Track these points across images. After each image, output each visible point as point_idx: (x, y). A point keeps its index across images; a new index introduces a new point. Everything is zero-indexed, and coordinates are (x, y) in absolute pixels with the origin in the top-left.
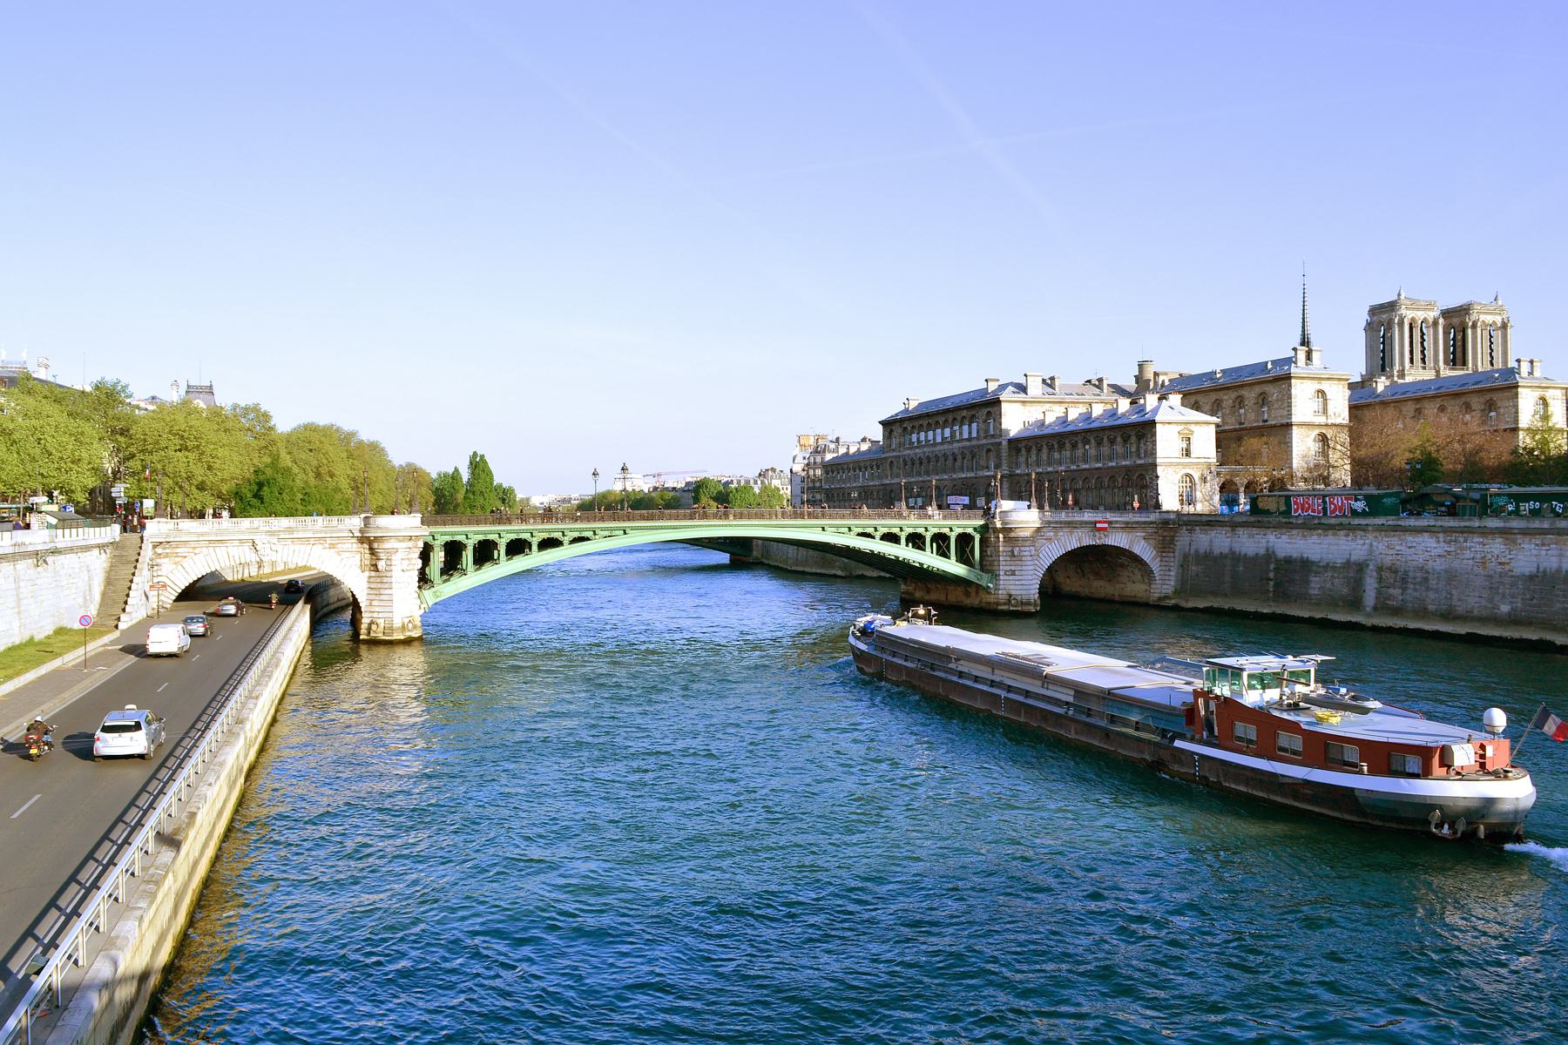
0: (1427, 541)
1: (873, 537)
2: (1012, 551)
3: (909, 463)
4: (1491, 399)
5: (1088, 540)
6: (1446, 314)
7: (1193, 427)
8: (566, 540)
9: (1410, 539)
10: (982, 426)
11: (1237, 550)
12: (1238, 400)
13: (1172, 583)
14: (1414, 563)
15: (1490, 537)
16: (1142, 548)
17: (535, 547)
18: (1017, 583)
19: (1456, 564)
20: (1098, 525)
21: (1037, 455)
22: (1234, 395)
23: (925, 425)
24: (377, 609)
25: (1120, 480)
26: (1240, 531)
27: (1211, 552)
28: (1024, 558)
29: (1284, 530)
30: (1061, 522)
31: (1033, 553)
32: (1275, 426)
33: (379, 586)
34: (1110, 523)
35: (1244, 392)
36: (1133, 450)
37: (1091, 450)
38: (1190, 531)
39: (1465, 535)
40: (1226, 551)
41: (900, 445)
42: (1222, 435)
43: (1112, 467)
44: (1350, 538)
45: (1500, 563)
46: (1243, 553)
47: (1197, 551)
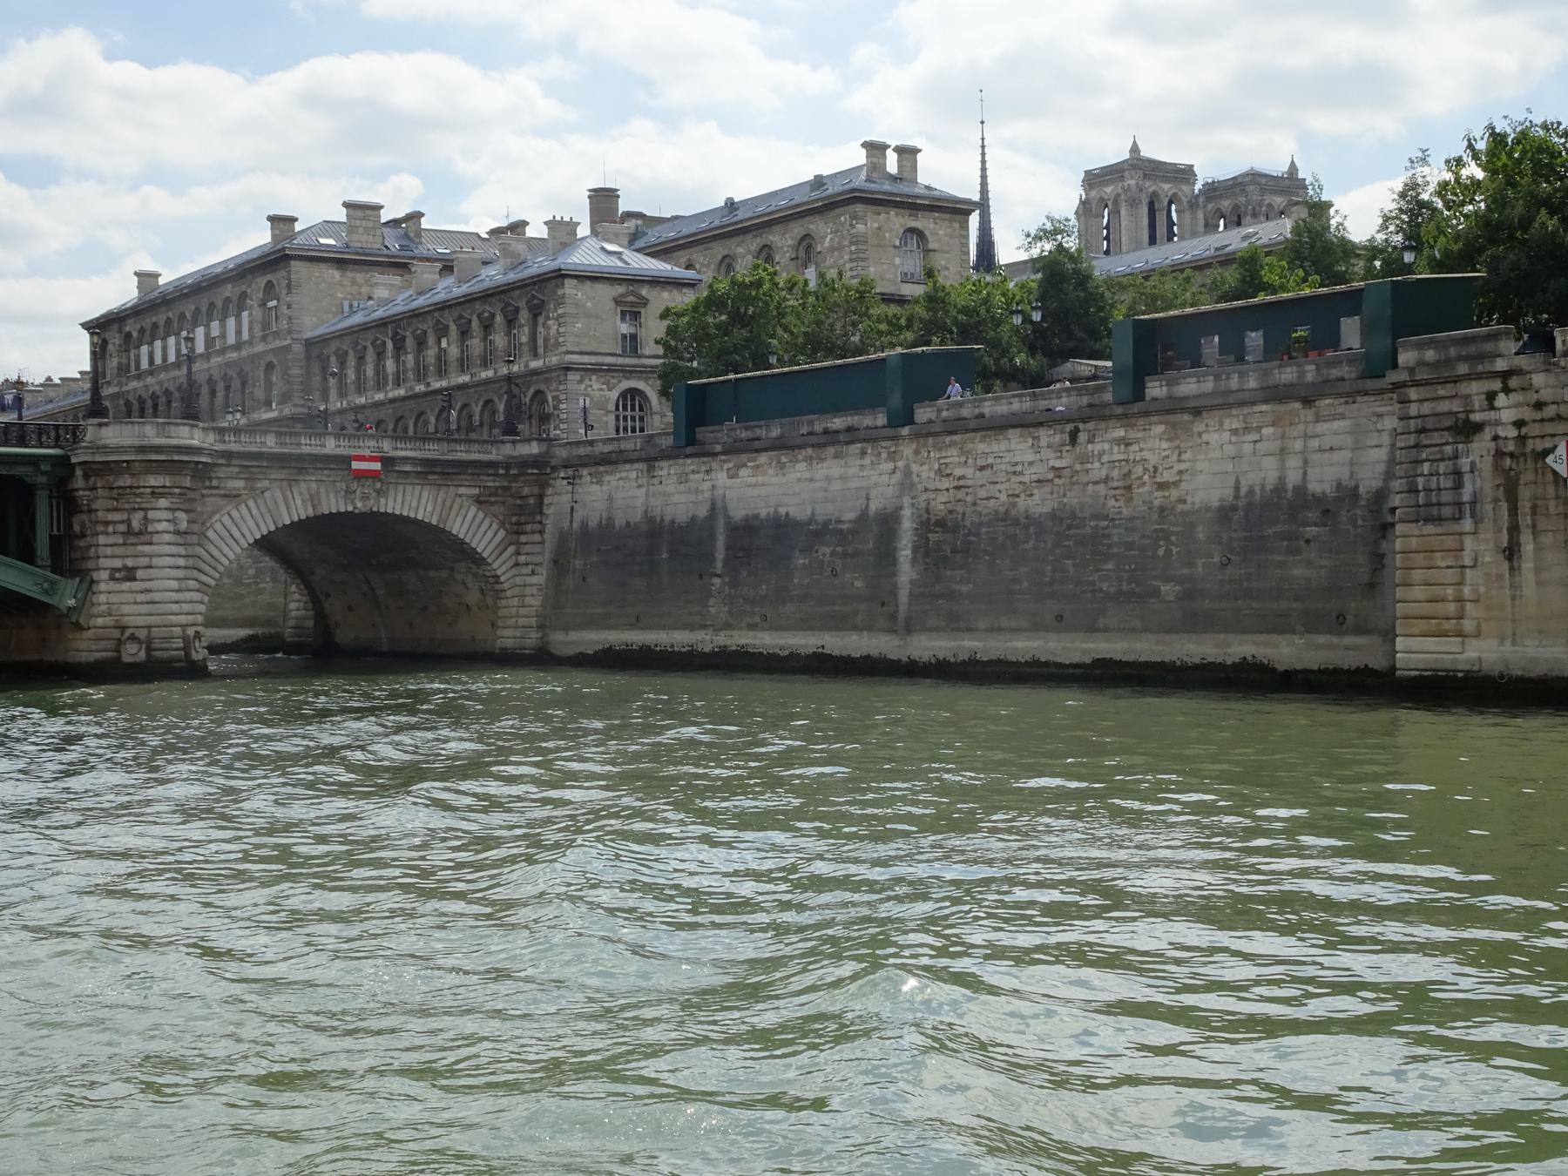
0: (1016, 448)
2: (128, 522)
5: (333, 503)
7: (644, 291)
9: (981, 447)
11: (657, 512)
12: (764, 254)
14: (992, 503)
15: (1141, 421)
18: (141, 598)
19: (1072, 499)
20: (355, 465)
22: (754, 244)
23: (161, 324)
26: (666, 469)
29: (744, 457)
30: (258, 456)
31: (183, 526)
34: (388, 462)
36: (524, 339)
39: (1091, 425)
40: (636, 516)
41: (123, 370)
43: (488, 382)
44: (867, 460)
45: (1162, 486)
46: (667, 519)
47: (584, 525)
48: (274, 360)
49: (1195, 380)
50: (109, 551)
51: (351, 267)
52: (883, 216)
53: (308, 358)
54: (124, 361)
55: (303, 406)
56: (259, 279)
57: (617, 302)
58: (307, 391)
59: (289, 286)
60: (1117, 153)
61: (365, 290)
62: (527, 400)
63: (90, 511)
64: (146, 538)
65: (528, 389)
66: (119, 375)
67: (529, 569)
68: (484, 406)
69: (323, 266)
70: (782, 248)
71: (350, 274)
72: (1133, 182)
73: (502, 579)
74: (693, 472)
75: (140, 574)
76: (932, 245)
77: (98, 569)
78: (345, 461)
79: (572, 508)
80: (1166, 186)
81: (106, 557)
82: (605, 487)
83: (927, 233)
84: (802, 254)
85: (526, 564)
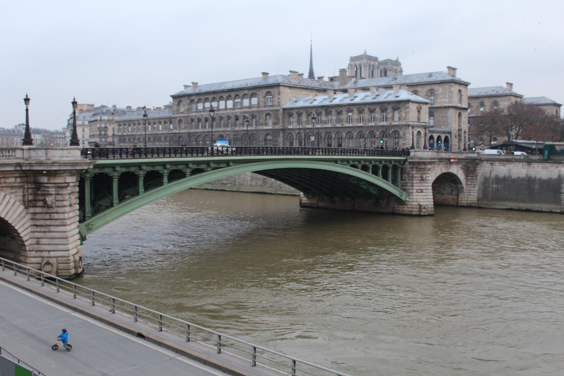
1: (357, 168)
2: (422, 177)
3: (196, 120)
4: (496, 101)
5: (444, 171)
6: (381, 63)
7: (421, 105)
8: (188, 171)
10: (262, 99)
11: (533, 176)
13: (476, 194)
16: (461, 175)
17: (165, 179)
18: (425, 197)
20: (452, 160)
21: (307, 118)
24: (47, 248)
25: (378, 133)
27: (510, 177)
28: (428, 181)
32: (440, 108)
33: (48, 222)
35: (419, 89)
37: (355, 115)
38: (491, 164)
41: (189, 110)
42: (433, 110)
48: (271, 113)
50: (416, 185)
53: (283, 113)
54: (190, 107)
57: (417, 108)
59: (279, 93)
60: (361, 53)
61: (295, 95)
62: (391, 132)
63: (409, 174)
64: (426, 181)
65: (391, 130)
67: (473, 186)
68: (369, 133)
72: (365, 61)
74: (550, 167)
75: (424, 191)
77: (413, 189)
78: (449, 159)
79: (491, 172)
84: (429, 94)
85: (471, 184)
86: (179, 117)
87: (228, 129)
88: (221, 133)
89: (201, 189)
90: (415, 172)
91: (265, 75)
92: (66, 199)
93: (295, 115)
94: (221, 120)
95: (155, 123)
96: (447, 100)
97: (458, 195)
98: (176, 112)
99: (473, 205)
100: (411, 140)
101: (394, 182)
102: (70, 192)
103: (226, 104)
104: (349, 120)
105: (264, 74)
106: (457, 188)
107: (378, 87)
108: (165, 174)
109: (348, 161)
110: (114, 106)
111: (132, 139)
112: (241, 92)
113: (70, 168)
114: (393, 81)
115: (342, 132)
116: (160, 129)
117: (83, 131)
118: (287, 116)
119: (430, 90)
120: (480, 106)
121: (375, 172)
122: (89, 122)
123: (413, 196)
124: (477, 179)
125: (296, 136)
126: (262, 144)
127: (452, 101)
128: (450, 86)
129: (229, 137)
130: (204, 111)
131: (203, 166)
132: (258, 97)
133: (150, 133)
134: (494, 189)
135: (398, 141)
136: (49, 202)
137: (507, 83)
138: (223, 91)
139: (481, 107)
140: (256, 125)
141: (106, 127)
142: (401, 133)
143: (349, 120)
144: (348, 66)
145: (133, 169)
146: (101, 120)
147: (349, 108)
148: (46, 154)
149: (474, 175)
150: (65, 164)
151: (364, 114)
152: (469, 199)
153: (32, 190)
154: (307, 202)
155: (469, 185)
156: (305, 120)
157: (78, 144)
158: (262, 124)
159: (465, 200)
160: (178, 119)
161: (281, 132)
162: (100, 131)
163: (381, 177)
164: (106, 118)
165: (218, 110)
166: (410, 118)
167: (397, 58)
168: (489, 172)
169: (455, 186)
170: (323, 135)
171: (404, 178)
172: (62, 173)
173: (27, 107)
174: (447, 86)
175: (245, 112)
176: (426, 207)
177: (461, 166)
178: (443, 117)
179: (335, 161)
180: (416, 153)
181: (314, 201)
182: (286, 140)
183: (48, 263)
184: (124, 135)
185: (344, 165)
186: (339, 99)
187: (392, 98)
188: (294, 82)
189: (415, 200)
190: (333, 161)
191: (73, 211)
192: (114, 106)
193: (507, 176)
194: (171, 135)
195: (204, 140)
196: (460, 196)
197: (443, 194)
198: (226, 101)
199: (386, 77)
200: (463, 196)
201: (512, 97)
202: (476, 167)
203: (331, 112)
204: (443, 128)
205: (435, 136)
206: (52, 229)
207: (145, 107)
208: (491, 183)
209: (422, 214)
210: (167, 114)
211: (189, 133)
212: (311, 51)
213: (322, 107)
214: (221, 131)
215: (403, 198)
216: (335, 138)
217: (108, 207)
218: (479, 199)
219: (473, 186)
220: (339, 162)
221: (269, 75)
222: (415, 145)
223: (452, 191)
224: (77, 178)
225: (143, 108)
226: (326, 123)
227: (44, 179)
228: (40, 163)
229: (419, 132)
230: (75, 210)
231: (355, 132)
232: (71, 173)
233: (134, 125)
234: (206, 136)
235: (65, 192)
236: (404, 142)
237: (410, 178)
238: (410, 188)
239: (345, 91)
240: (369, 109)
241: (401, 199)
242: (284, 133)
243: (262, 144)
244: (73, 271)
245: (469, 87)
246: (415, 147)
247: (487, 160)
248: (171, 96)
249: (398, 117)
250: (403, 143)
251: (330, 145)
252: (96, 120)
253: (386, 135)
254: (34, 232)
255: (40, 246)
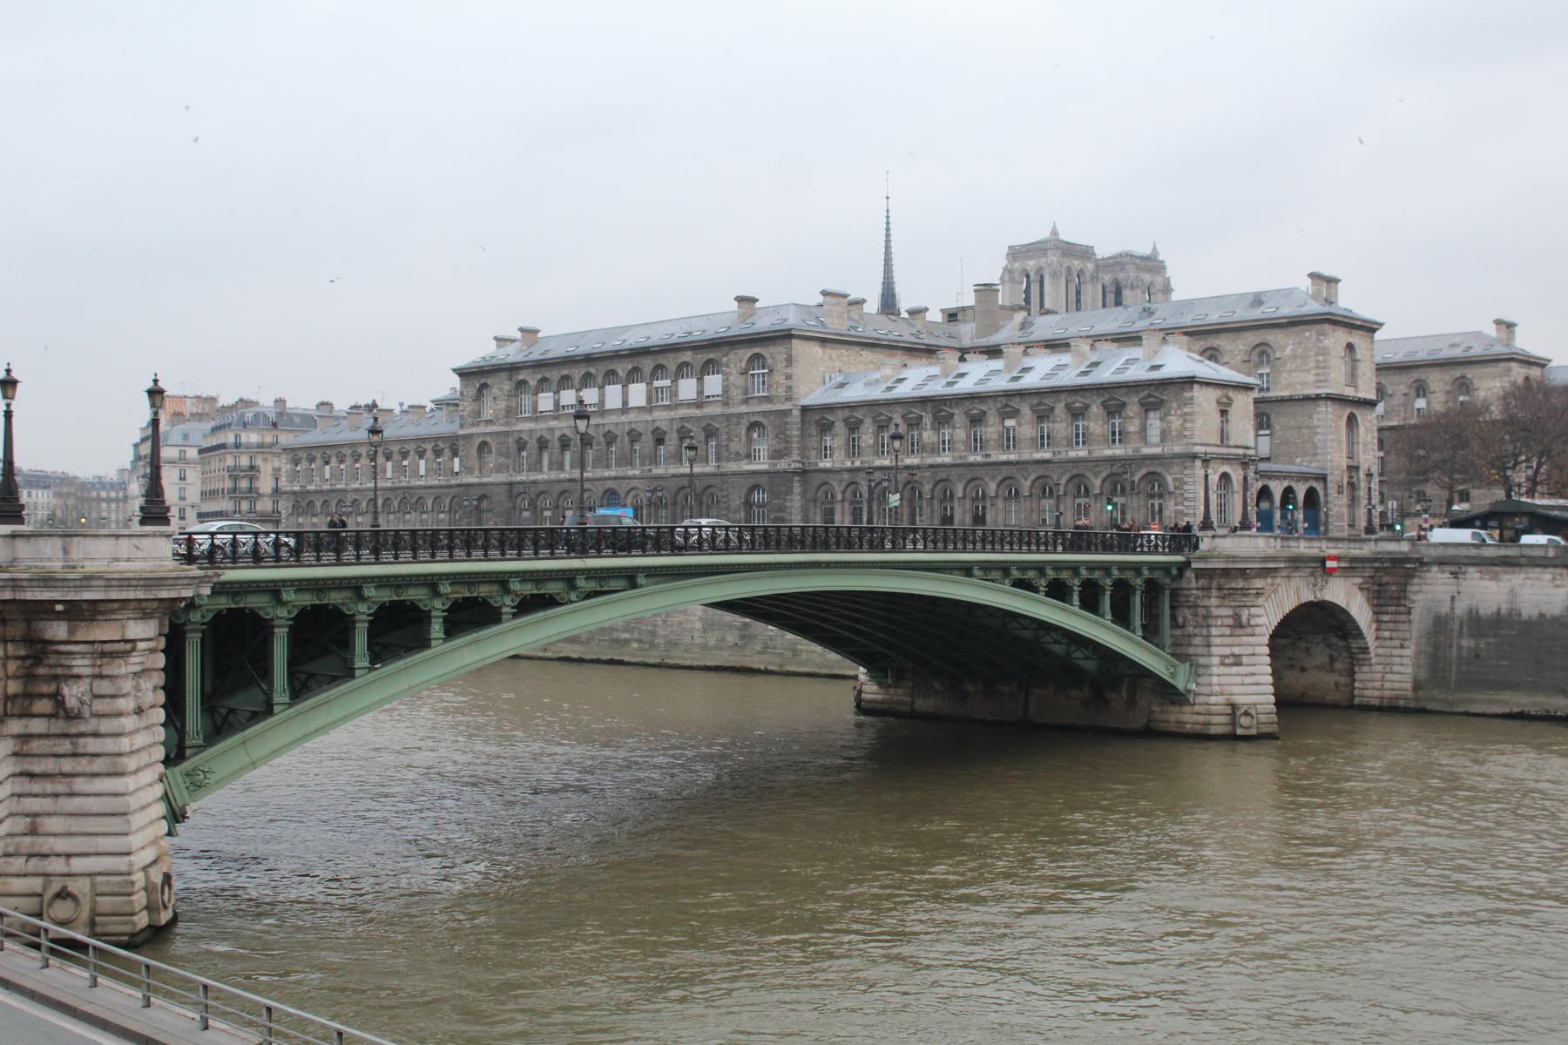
1: (1036, 591)
2: (1237, 617)
4: (1463, 377)
5: (1307, 596)
7: (1231, 394)
8: (507, 603)
10: (736, 379)
13: (1410, 670)
16: (1359, 610)
17: (437, 629)
18: (1248, 680)
20: (1329, 564)
21: (876, 436)
24: (61, 845)
25: (1098, 482)
28: (1258, 630)
32: (1291, 400)
33: (67, 765)
35: (1222, 342)
38: (1455, 575)
41: (509, 412)
43: (1076, 462)
49: (1355, 446)
50: (1218, 641)
51: (829, 345)
52: (1336, 334)
53: (803, 421)
54: (514, 404)
55: (799, 462)
56: (741, 352)
57: (1218, 403)
58: (804, 450)
59: (789, 361)
60: (1040, 233)
62: (1137, 478)
63: (1197, 606)
64: (1249, 630)
65: (1138, 470)
66: (507, 416)
67: (1397, 643)
69: (812, 344)
70: (1232, 351)
71: (828, 351)
72: (1055, 259)
73: (1371, 649)
75: (1245, 660)
76: (1359, 356)
78: (1323, 560)
79: (1453, 598)
80: (1076, 263)
81: (1216, 646)
82: (1501, 584)
83: (1356, 347)
84: (1255, 358)
85: (1391, 639)
86: (479, 435)
87: (630, 473)
88: (610, 484)
89: (548, 659)
90: (1214, 601)
91: (746, 305)
92: (124, 692)
93: (840, 428)
94: (609, 444)
95: (405, 455)
96: (1311, 378)
97: (1352, 673)
98: (470, 420)
99: (1402, 703)
100: (1202, 500)
101: (1151, 632)
102: (137, 668)
103: (625, 394)
104: (1008, 440)
105: (741, 300)
106: (1348, 649)
107: (1096, 339)
108: (434, 613)
109: (1004, 568)
110: (280, 402)
111: (334, 503)
112: (670, 356)
113: (140, 595)
114: (1140, 319)
115: (987, 479)
116: (422, 471)
117: (183, 478)
118: (813, 430)
119: (1259, 345)
120: (1413, 393)
121: (1090, 603)
122: (201, 451)
123: (1211, 675)
124: (1410, 621)
125: (844, 492)
126: (738, 516)
127: (1325, 381)
128: (1319, 334)
129: (636, 496)
130: (556, 418)
131: (553, 588)
132: (724, 374)
133: (389, 484)
134: (1464, 653)
135: (1160, 505)
136: (71, 702)
137: (1498, 322)
138: (617, 355)
139: (1418, 396)
140: (718, 459)
141: (252, 468)
142: (1169, 479)
143: (1008, 440)
144: (1003, 274)
145: (335, 598)
146: (237, 446)
147: (1007, 406)
148: (66, 551)
149: (1402, 609)
150: (125, 582)
151: (1054, 422)
152: (1387, 685)
153: (19, 662)
154: (880, 697)
155: (1385, 639)
156: (871, 442)
157: (165, 521)
158: (738, 454)
159: (1373, 689)
160: (478, 441)
161: (796, 478)
162: (235, 479)
163: (1109, 617)
164: (253, 438)
165: (602, 411)
166: (1197, 433)
167: (1155, 248)
168: (1448, 598)
169: (1341, 643)
170: (927, 487)
171: (1180, 620)
172: (113, 611)
173: (8, 405)
174: (1309, 333)
175: (682, 419)
176: (1253, 712)
177: (1359, 581)
178: (1300, 428)
179: (966, 570)
180: (1218, 541)
181: (900, 695)
182: (812, 505)
183: (63, 894)
184: (309, 492)
185: (993, 581)
186: (977, 375)
187: (1137, 373)
188: (836, 324)
189: (1216, 688)
190: (957, 569)
191: (147, 728)
192: (280, 402)
193: (1503, 611)
194: (456, 490)
195: (557, 507)
196: (1357, 676)
197: (1303, 670)
198: (625, 387)
199: (1120, 309)
200: (1368, 676)
201: (1513, 364)
202: (1406, 585)
203: (952, 415)
204: (1300, 465)
205: (1277, 488)
206: (80, 784)
207: (375, 405)
208: (1455, 635)
209: (1239, 731)
210: (444, 425)
211: (511, 484)
212: (888, 230)
213: (924, 401)
214: (610, 478)
215: (1180, 684)
216: (964, 497)
217: (255, 717)
218: (1417, 686)
219: (1397, 643)
220: (977, 572)
221: (758, 305)
222: (1214, 517)
223: (1332, 660)
224: (161, 625)
225: (367, 406)
226: (934, 450)
227: (59, 630)
228: (47, 580)
229: (1225, 477)
230: (154, 725)
231: (1026, 479)
232: (143, 610)
233: (341, 462)
234: (562, 493)
235: (123, 671)
236: (1180, 508)
237: (1200, 620)
238: (1201, 650)
239: (993, 352)
240: (1068, 406)
241: (1175, 688)
242: (804, 484)
243: (738, 516)
244: (142, 920)
245: (1378, 336)
246: (1215, 524)
247: (1441, 562)
248: (454, 370)
249: (1158, 432)
250: (1176, 511)
251: (947, 519)
252: (222, 446)
253: (1122, 487)
254: (20, 796)
255: (40, 840)
